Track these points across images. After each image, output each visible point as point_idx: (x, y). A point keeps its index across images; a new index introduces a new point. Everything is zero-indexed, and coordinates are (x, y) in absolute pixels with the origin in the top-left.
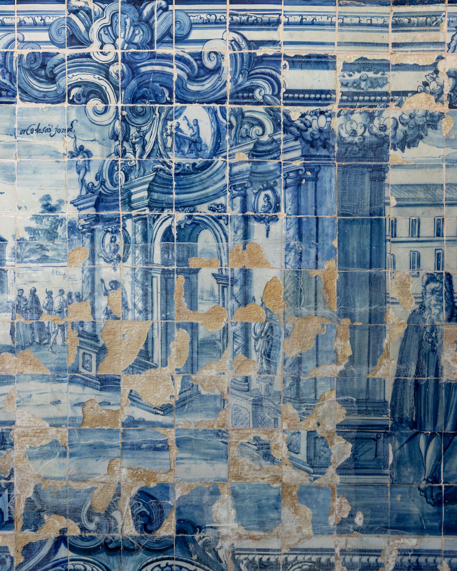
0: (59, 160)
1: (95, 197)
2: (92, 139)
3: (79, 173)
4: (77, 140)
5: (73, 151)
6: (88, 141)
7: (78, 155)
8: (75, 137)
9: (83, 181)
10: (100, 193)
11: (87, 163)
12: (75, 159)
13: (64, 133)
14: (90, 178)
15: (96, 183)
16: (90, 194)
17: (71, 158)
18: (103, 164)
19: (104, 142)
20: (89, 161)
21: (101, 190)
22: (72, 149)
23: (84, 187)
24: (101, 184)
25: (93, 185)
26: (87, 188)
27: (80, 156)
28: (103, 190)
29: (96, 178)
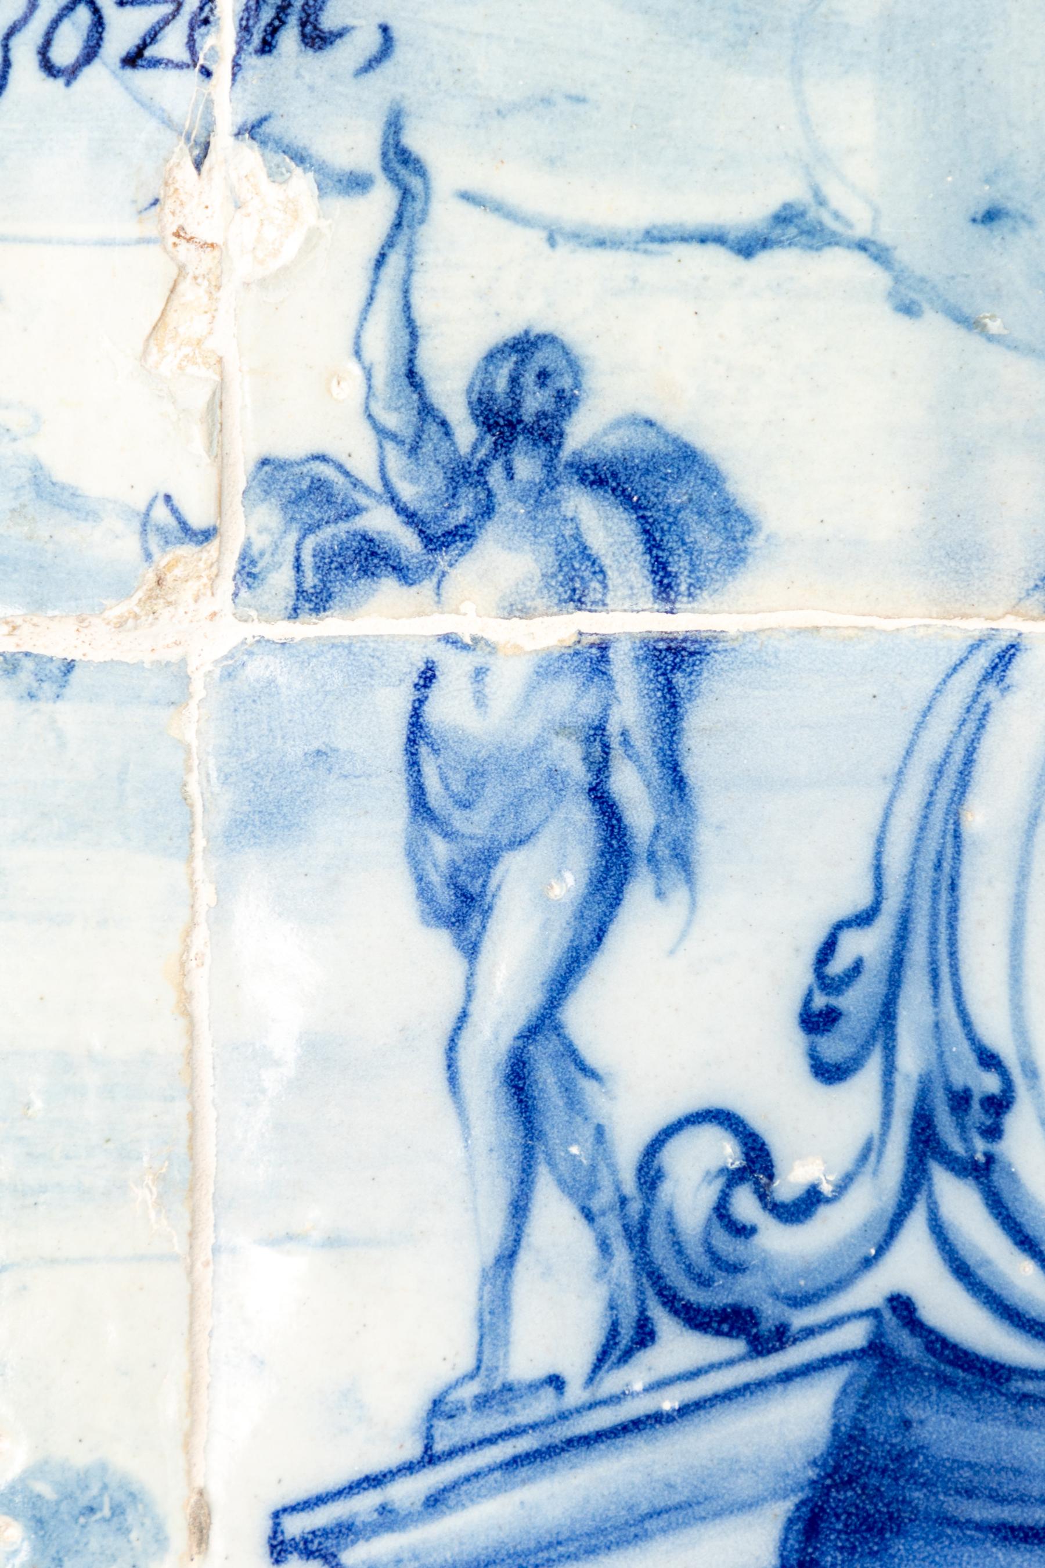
0: (55, 639)
1: (798, 1421)
2: (747, 209)
3: (462, 907)
4: (446, 222)
5: (361, 455)
6: (657, 237)
7: (445, 539)
8: (400, 161)
9: (535, 1079)
10: (904, 1354)
11: (630, 708)
12: (387, 617)
13: (171, 89)
14: (693, 1014)
15: (823, 1132)
16: (678, 1347)
17: (313, 600)
18: (977, 718)
19: (1008, 259)
20: (673, 662)
21: (912, 1267)
22: (333, 418)
23: (556, 1222)
24: (924, 1142)
25: (757, 1161)
26: (635, 1226)
27: (502, 562)
28: (962, 1270)
29: (816, 1021)
